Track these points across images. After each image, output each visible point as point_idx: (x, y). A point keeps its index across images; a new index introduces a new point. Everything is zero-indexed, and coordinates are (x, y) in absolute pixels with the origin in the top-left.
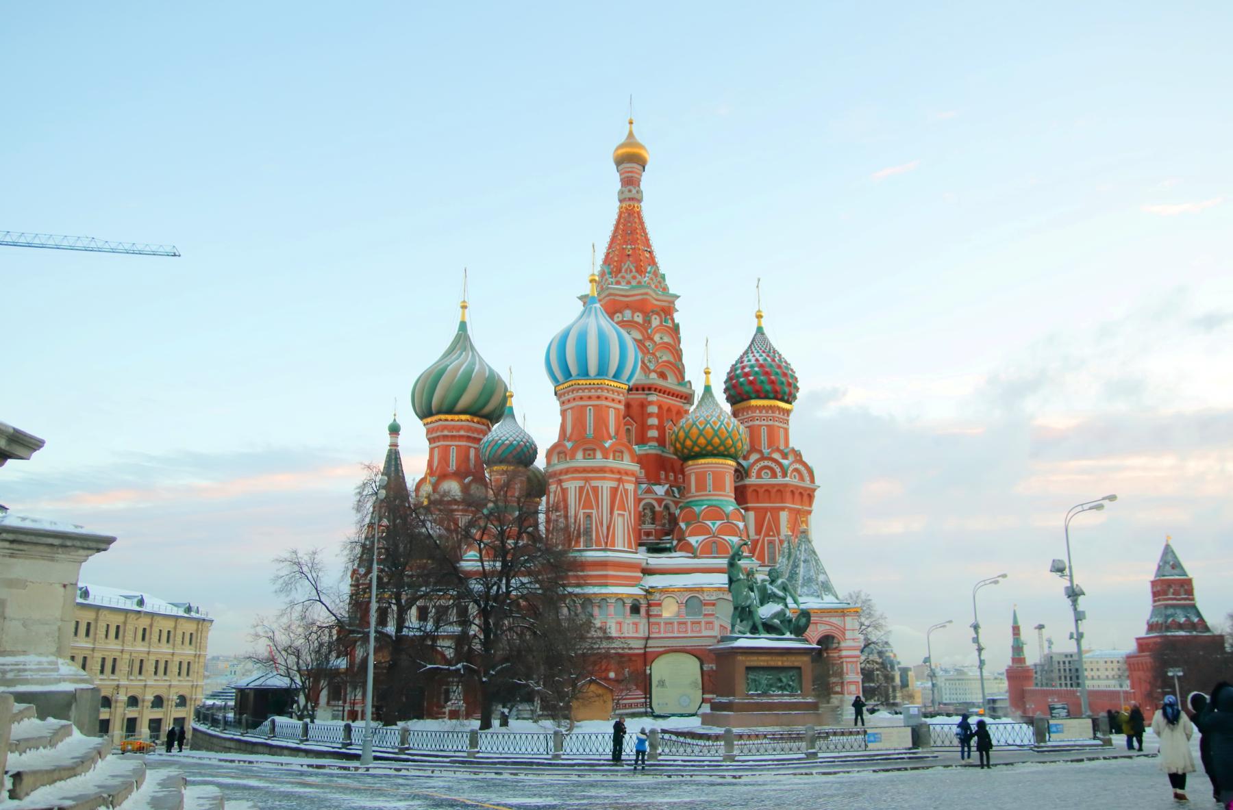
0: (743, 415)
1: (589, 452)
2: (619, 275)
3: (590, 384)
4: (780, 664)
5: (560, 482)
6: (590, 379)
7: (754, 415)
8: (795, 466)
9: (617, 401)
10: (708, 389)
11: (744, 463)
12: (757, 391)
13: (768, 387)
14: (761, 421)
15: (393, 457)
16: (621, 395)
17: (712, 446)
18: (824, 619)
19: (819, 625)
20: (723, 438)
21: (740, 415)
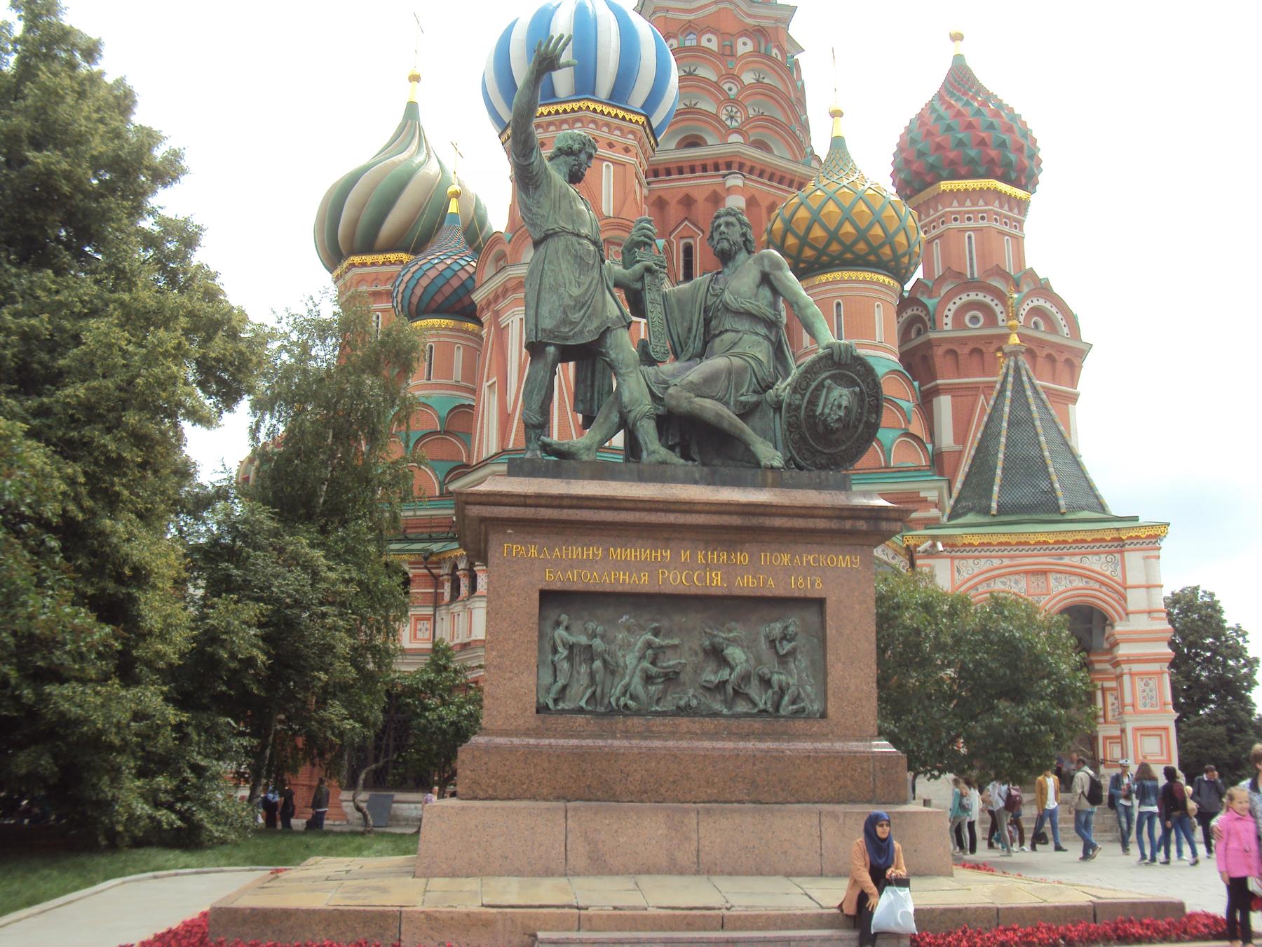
0: (928, 216)
3: (557, 112)
4: (716, 582)
5: (497, 314)
6: (556, 103)
8: (1036, 303)
9: (619, 148)
10: (837, 144)
11: (930, 303)
12: (952, 162)
13: (972, 153)
14: (962, 221)
16: (630, 136)
17: (841, 243)
18: (1066, 560)
19: (1052, 577)
20: (863, 226)
21: (923, 217)
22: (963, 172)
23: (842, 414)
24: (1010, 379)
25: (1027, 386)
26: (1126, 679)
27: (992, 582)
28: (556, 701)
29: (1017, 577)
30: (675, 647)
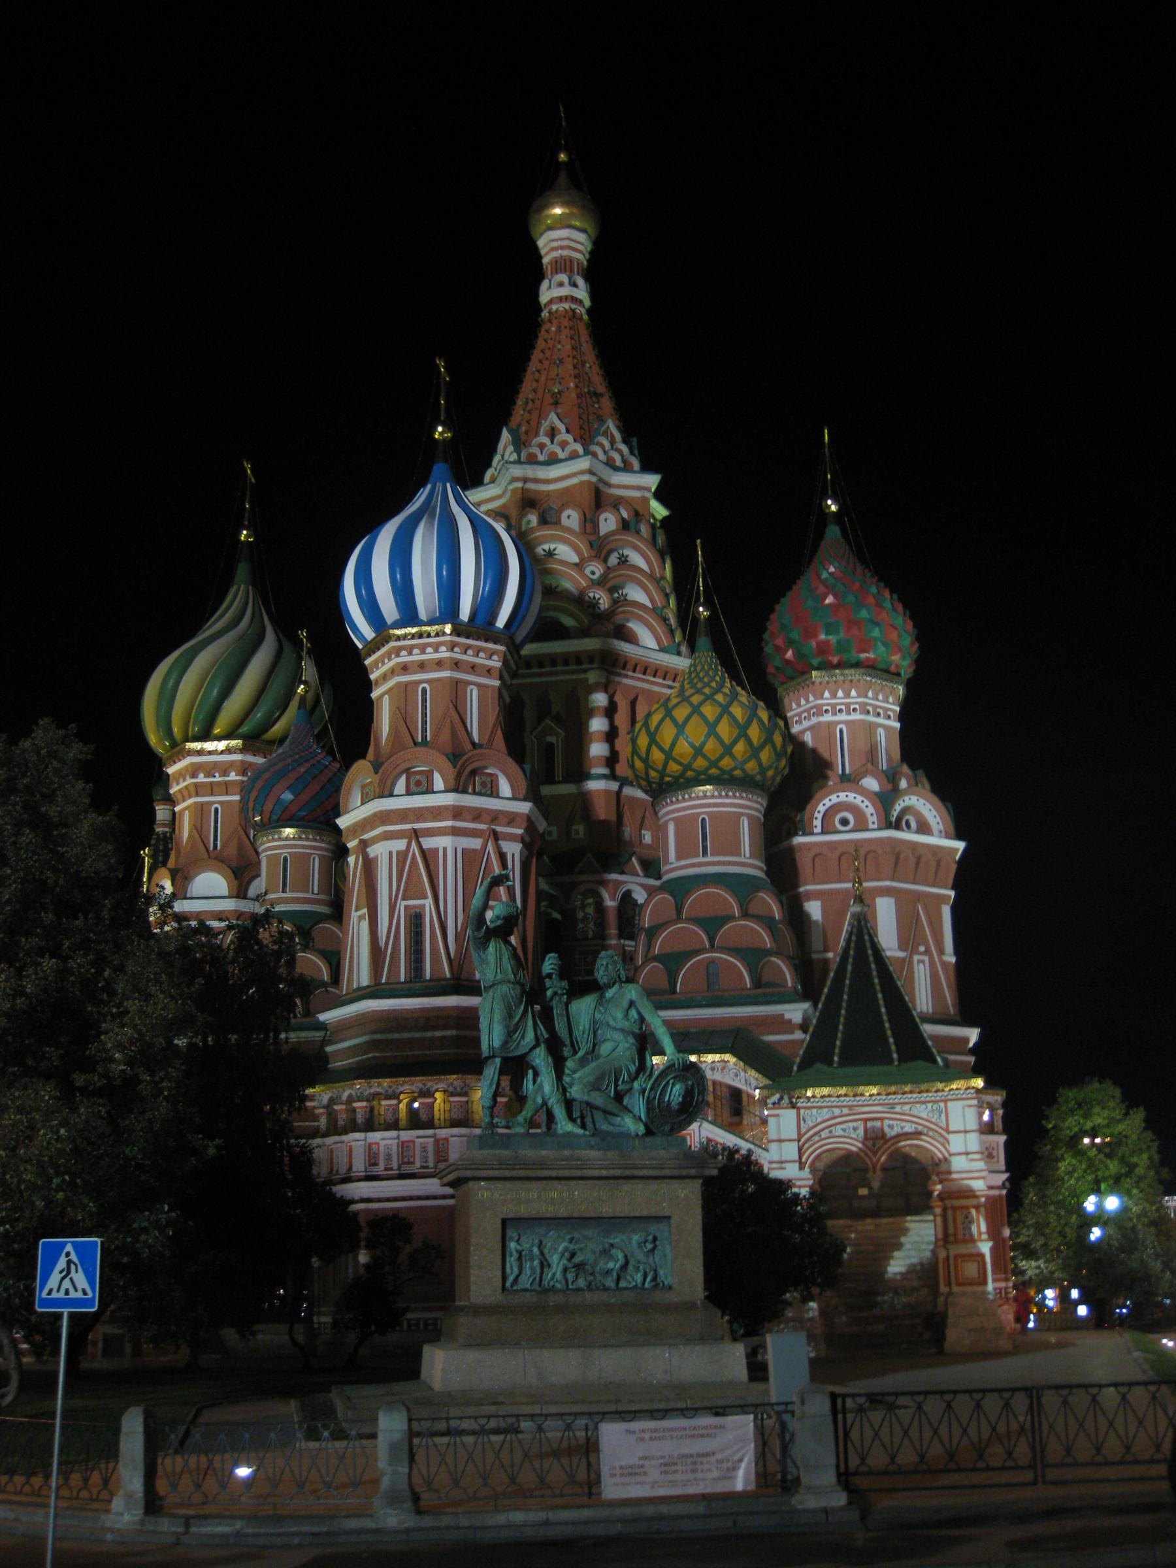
1: (418, 777)
2: (536, 441)
4: (607, 1210)
5: (364, 844)
7: (820, 702)
14: (834, 714)
15: (161, 847)
16: (495, 657)
17: (704, 757)
18: (898, 1109)
19: (886, 1122)
21: (794, 706)
22: (835, 660)
23: (680, 1099)
24: (854, 938)
25: (868, 945)
26: (950, 1213)
27: (833, 1128)
28: (512, 1285)
29: (855, 1124)
30: (581, 1249)
